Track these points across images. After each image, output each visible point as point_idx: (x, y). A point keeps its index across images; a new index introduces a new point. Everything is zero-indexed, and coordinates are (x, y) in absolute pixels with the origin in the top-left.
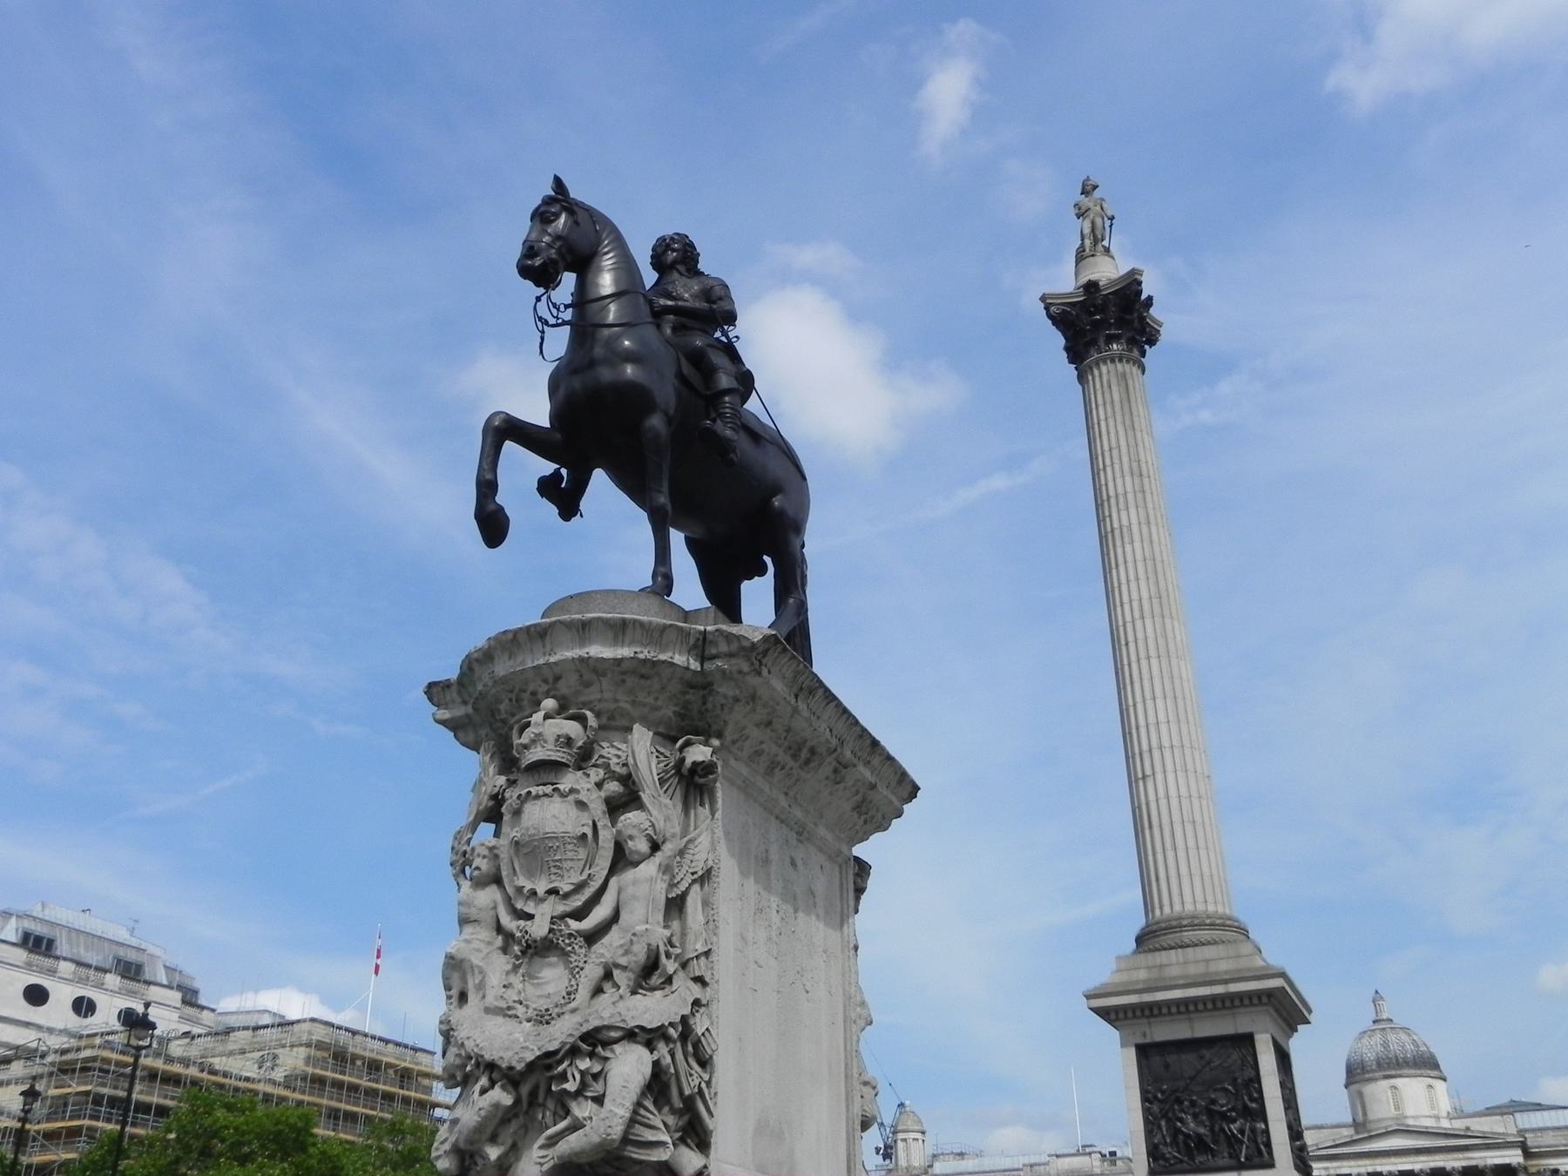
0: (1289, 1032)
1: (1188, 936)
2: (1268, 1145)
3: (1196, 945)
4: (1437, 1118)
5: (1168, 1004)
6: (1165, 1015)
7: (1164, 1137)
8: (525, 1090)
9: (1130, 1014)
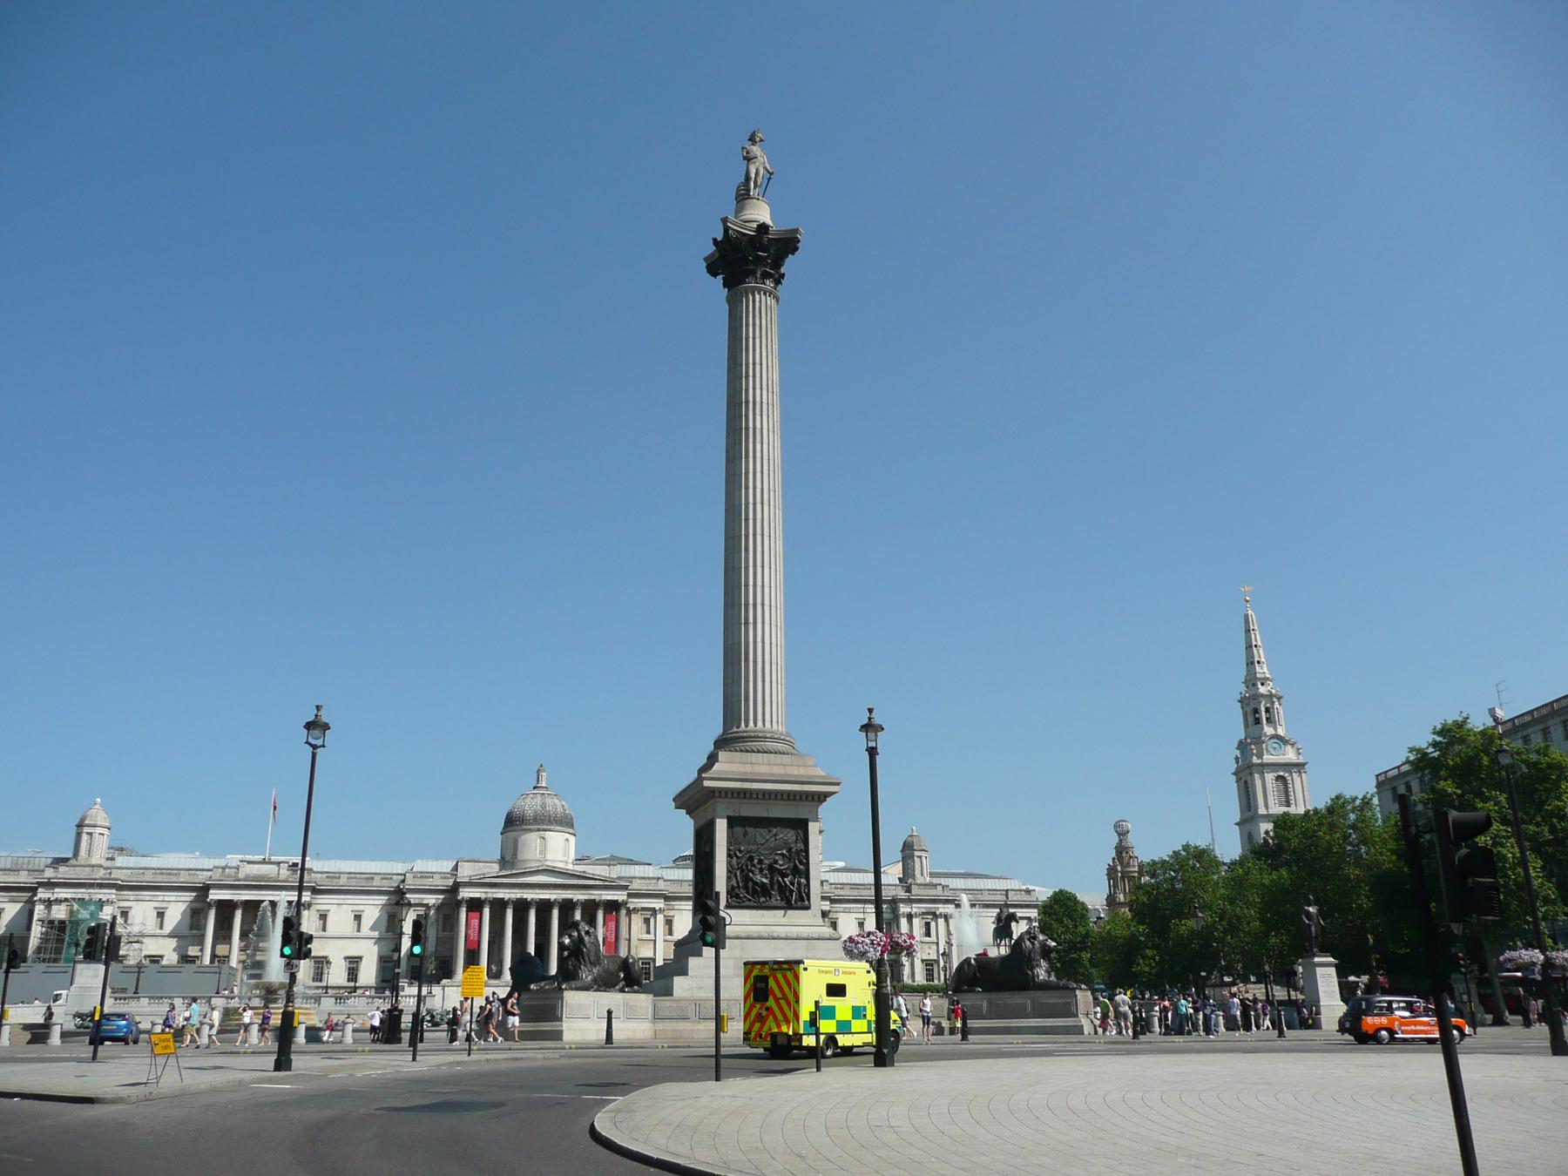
1: (770, 745)
2: (808, 895)
5: (758, 792)
7: (738, 882)
9: (730, 795)
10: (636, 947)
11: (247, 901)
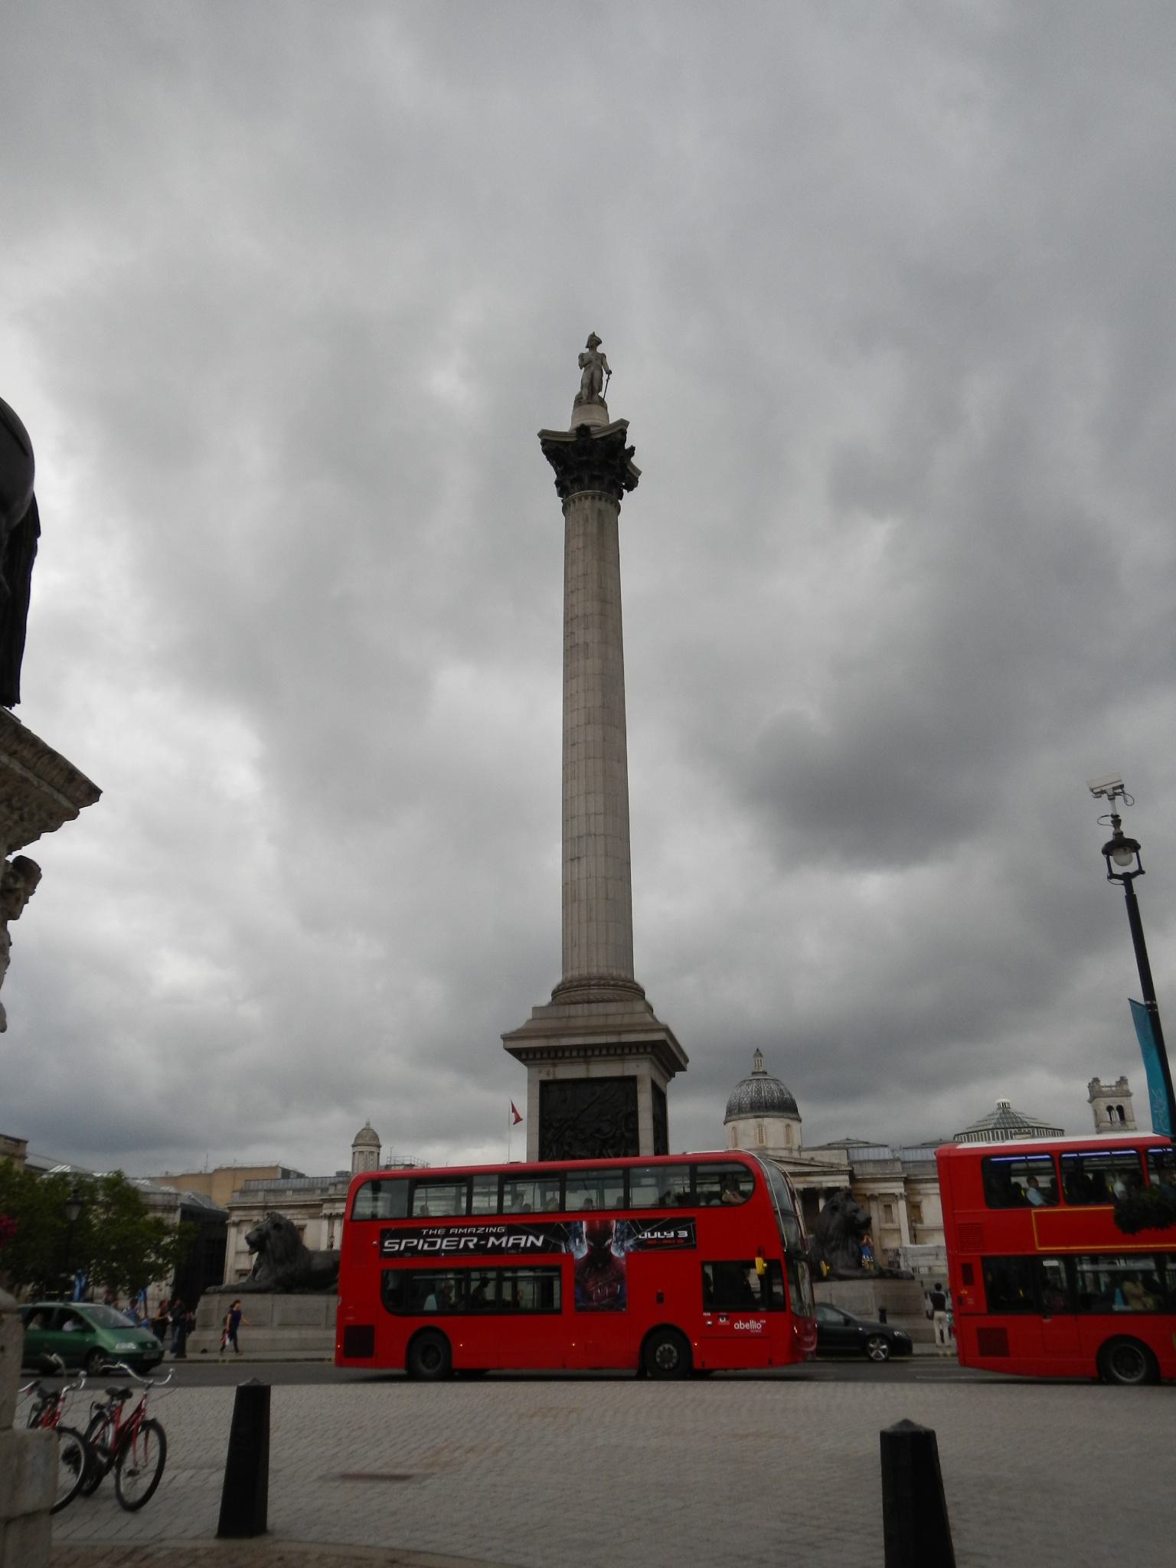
0: (666, 1075)
3: (600, 1002)
4: (791, 1150)
5: (571, 1048)
6: (574, 1057)
10: (880, 1239)
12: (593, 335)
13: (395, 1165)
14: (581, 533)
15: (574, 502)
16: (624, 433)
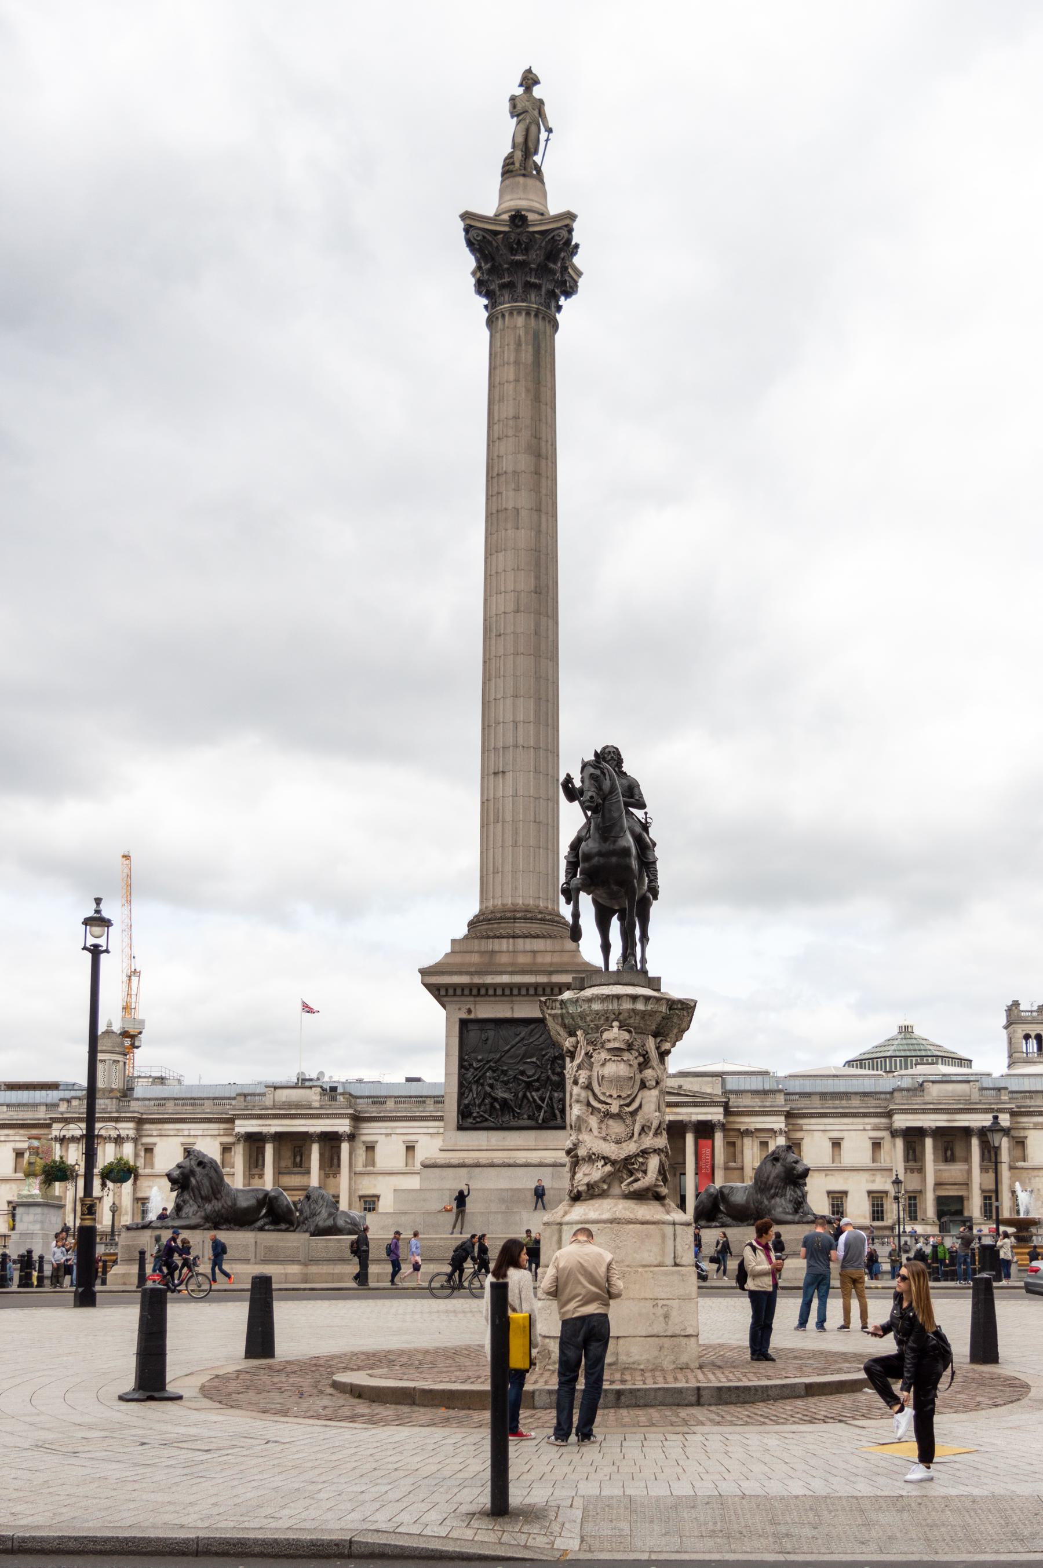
8: (618, 1167)
11: (276, 1133)
12: (529, 71)
13: (140, 1077)
14: (512, 360)
15: (503, 316)
16: (570, 231)
